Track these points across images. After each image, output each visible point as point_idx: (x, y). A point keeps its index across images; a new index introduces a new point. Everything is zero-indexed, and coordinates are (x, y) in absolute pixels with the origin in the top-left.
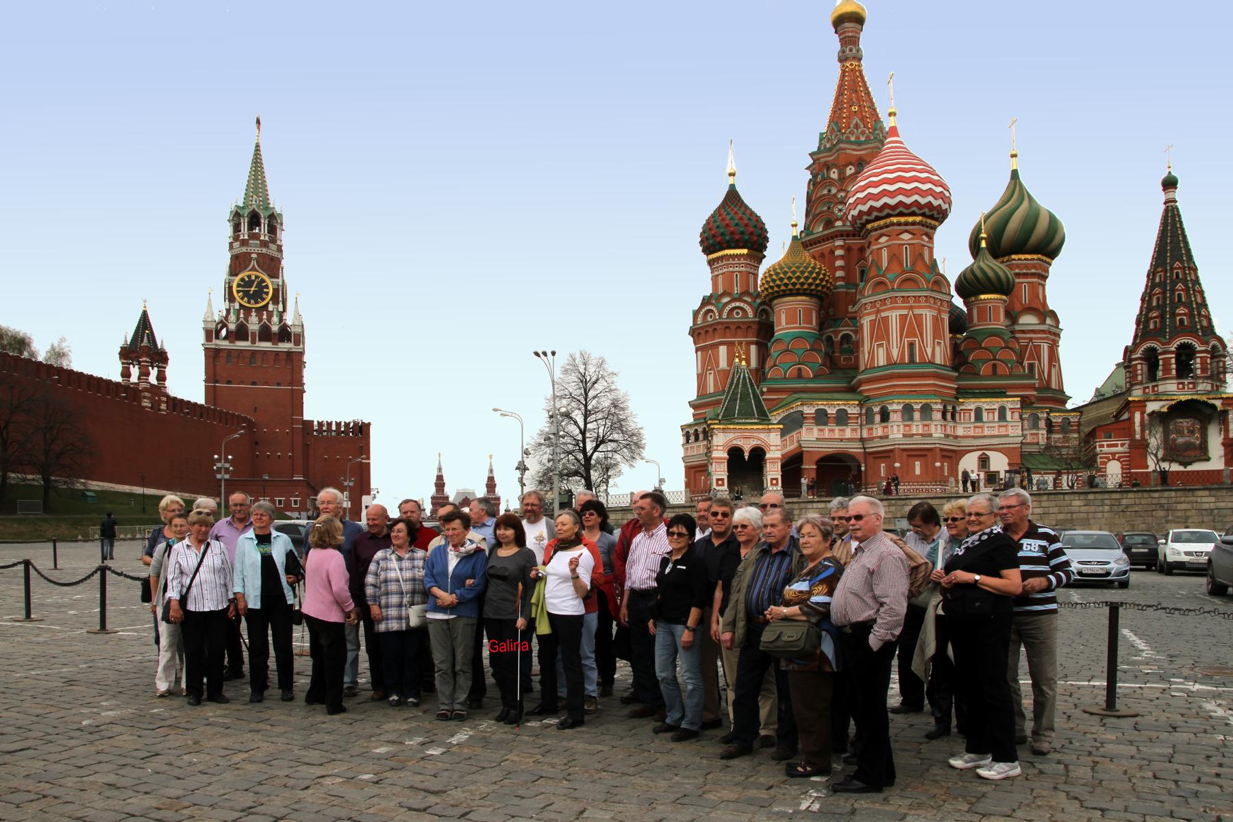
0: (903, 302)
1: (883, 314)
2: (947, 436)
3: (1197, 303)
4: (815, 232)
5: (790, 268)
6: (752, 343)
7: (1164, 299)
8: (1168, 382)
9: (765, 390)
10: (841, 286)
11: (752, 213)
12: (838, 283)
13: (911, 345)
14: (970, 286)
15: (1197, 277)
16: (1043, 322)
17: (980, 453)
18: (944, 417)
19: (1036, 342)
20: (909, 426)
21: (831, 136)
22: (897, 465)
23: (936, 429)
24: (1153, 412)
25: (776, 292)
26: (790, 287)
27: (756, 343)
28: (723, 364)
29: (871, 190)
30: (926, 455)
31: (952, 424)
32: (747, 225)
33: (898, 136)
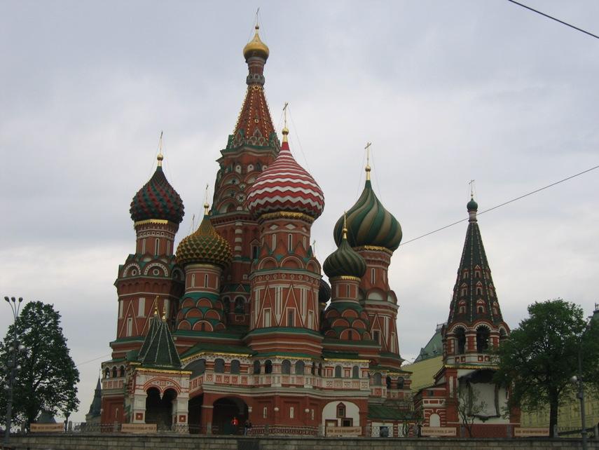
0: (286, 278)
4: (221, 212)
5: (201, 241)
6: (165, 297)
7: (469, 292)
8: (472, 355)
11: (173, 192)
13: (291, 313)
14: (334, 265)
15: (491, 277)
16: (385, 300)
17: (339, 402)
18: (313, 372)
21: (238, 138)
22: (277, 409)
23: (307, 381)
24: (462, 378)
25: (189, 259)
27: (169, 298)
28: (141, 313)
30: (298, 403)
31: (318, 378)
33: (289, 150)
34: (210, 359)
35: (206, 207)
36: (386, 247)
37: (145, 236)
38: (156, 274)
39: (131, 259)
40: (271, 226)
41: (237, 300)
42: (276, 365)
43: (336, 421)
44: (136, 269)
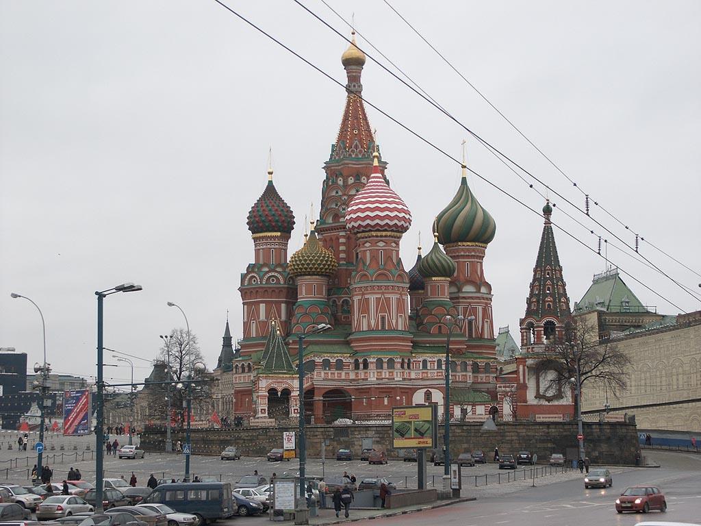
0: (378, 290)
1: (366, 297)
2: (404, 379)
4: (327, 222)
6: (282, 302)
9: (291, 341)
12: (341, 262)
13: (383, 318)
14: (426, 269)
16: (479, 291)
18: (402, 367)
19: (473, 305)
20: (381, 372)
27: (285, 302)
29: (359, 214)
31: (407, 371)
32: (277, 210)
34: (318, 360)
35: (312, 223)
38: (273, 282)
39: (251, 268)
40: (365, 243)
41: (343, 302)
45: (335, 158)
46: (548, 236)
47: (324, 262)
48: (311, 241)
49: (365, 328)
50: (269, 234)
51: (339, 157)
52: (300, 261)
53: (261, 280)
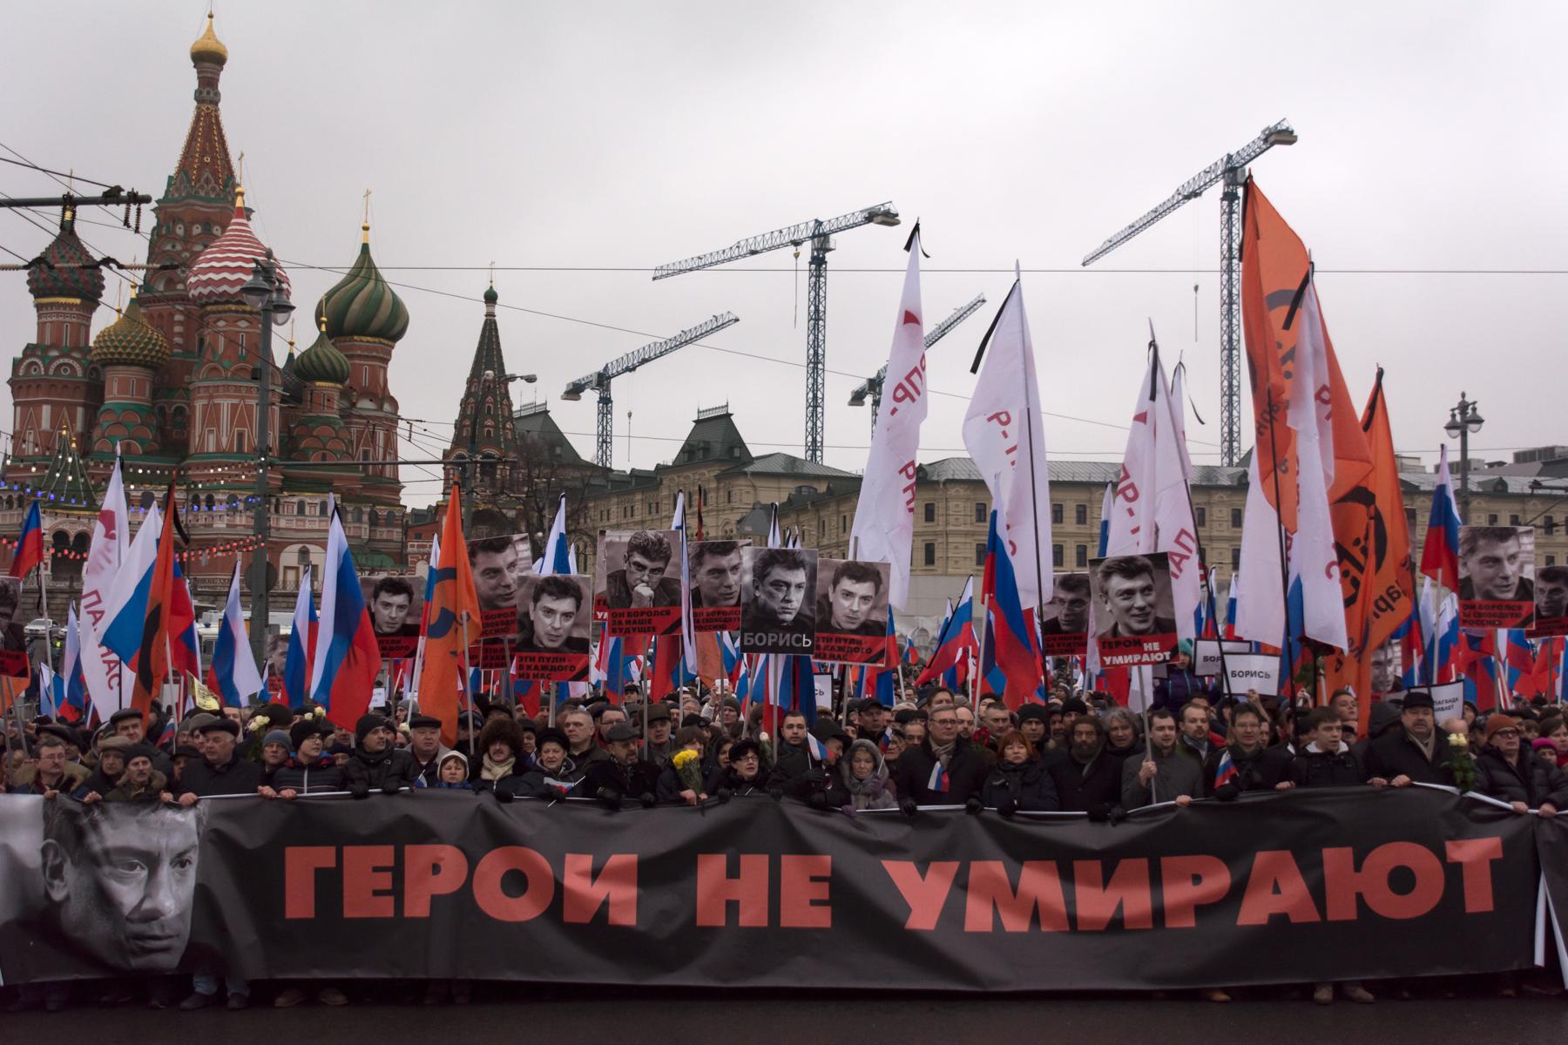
0: (235, 391)
1: (217, 401)
3: (503, 416)
6: (77, 404)
10: (178, 354)
12: (176, 350)
13: (241, 435)
14: (305, 370)
16: (381, 408)
17: (300, 546)
21: (181, 184)
26: (124, 356)
27: (84, 405)
31: (276, 516)
36: (384, 338)
37: (49, 319)
39: (30, 350)
40: (219, 319)
42: (221, 502)
43: (296, 569)
44: (35, 363)
45: (173, 195)
46: (490, 332)
47: (150, 346)
48: (129, 317)
49: (212, 448)
50: (63, 300)
51: (180, 194)
52: (112, 341)
53: (47, 370)
